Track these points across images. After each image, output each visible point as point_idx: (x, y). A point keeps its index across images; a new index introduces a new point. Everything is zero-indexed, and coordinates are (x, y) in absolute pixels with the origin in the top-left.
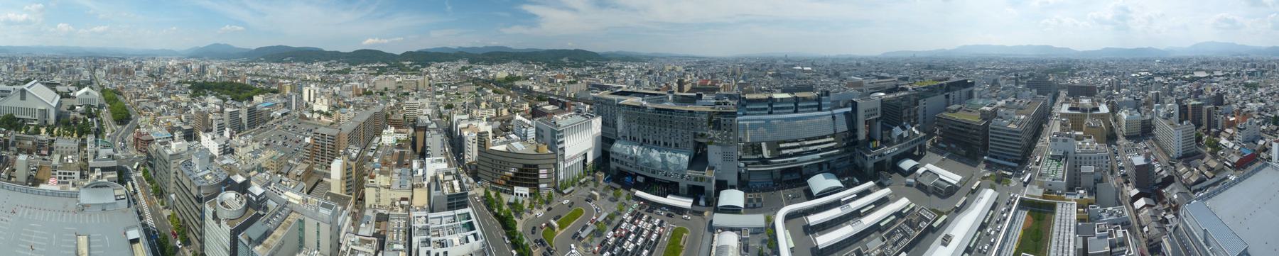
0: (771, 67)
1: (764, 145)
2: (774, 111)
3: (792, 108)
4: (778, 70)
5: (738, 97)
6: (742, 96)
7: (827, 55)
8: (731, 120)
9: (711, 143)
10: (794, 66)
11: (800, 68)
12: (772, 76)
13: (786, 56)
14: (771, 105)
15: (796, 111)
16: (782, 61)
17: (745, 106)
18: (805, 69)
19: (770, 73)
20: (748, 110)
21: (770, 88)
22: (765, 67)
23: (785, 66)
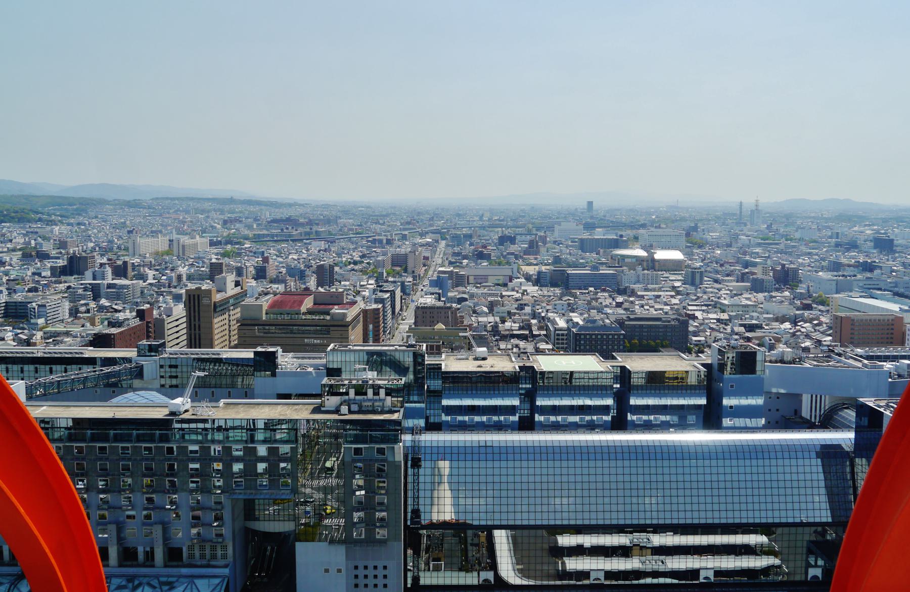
0: (533, 248)
1: (501, 538)
2: (538, 418)
3: (605, 409)
4: (557, 260)
5: (408, 360)
6: (429, 360)
7: (749, 200)
8: (381, 451)
9: (309, 534)
10: (616, 244)
11: (642, 253)
12: (538, 281)
13: (590, 204)
14: (530, 397)
15: (619, 424)
16: (572, 225)
17: (436, 395)
18: (660, 255)
19: (532, 270)
20: (449, 410)
21: (529, 327)
22: (513, 248)
23: (583, 245)
